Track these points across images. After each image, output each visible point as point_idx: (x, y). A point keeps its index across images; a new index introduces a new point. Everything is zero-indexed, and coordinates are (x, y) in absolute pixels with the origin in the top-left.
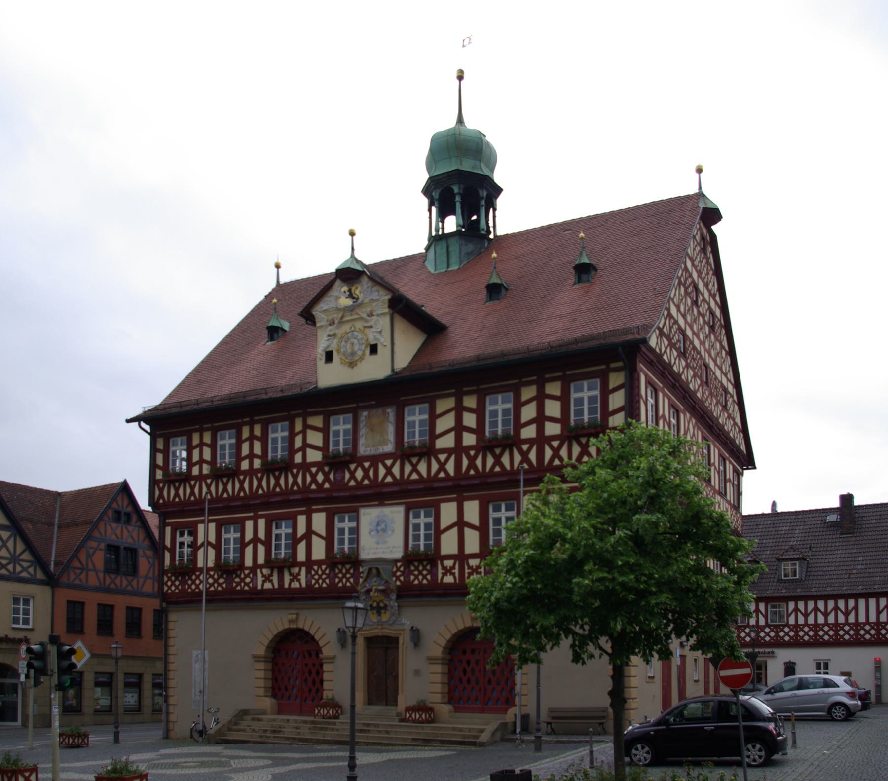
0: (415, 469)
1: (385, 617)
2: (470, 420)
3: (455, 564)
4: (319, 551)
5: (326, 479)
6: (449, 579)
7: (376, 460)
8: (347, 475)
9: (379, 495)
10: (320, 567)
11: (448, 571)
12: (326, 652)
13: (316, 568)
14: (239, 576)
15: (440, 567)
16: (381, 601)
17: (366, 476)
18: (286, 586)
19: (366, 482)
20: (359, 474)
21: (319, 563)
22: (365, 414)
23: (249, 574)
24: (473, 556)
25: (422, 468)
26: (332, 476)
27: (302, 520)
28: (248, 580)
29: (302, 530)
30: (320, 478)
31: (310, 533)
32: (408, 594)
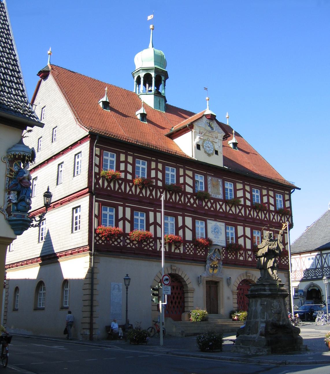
0: (230, 209)
1: (216, 271)
2: (248, 195)
3: (243, 252)
4: (189, 236)
5: (195, 202)
6: (241, 258)
7: (216, 200)
8: (204, 204)
9: (217, 216)
10: (190, 244)
11: (241, 255)
12: (189, 286)
13: (188, 244)
14: (146, 242)
15: (238, 253)
16: (215, 264)
17: (212, 206)
18: (173, 251)
19: (212, 209)
20: (209, 205)
21: (189, 242)
22: (210, 178)
23: (152, 241)
24: (249, 250)
25: (233, 209)
26: (197, 202)
27: (180, 218)
28: (151, 245)
29: (180, 224)
30: (192, 201)
31: (184, 226)
32: (227, 263)
